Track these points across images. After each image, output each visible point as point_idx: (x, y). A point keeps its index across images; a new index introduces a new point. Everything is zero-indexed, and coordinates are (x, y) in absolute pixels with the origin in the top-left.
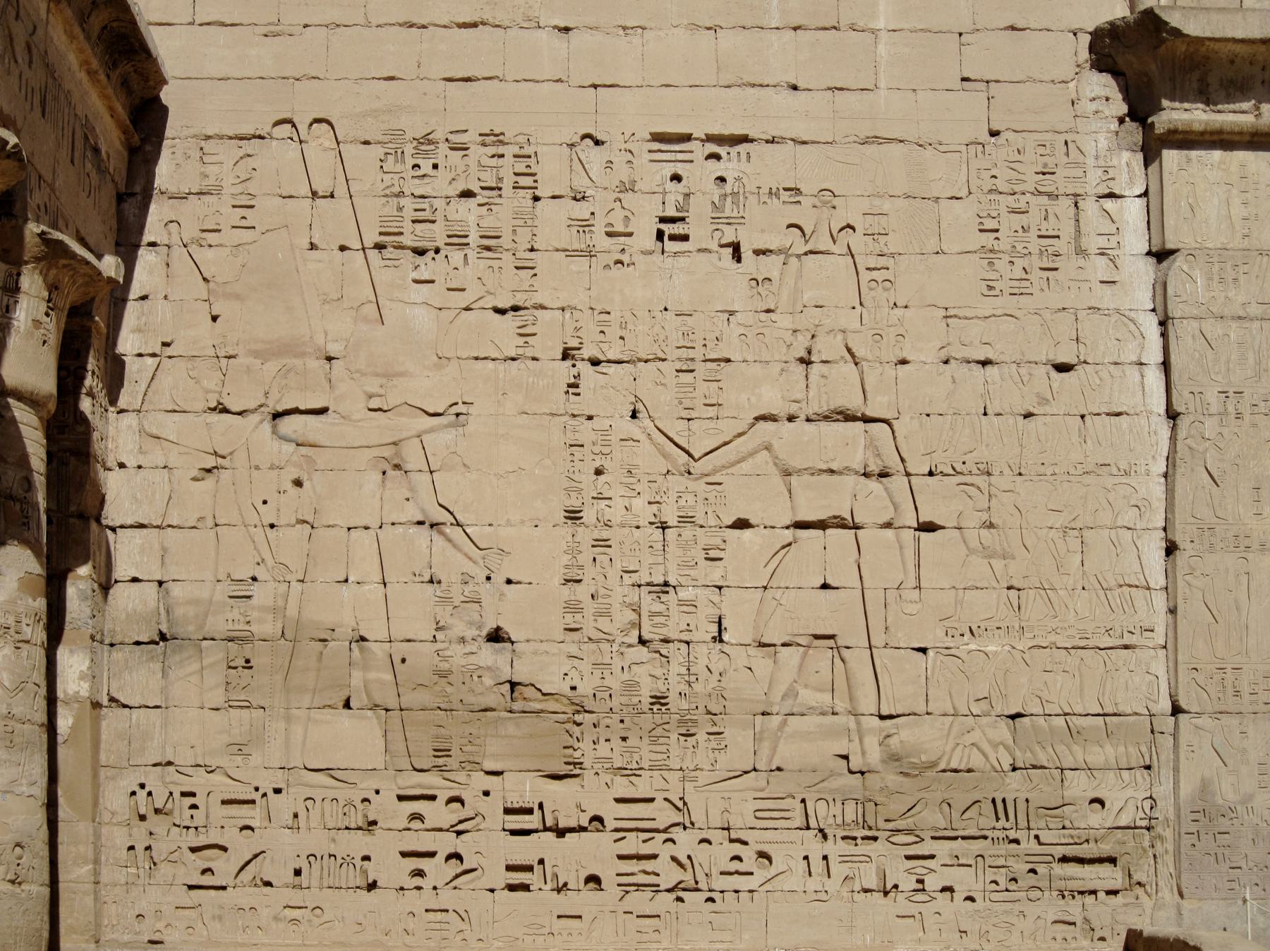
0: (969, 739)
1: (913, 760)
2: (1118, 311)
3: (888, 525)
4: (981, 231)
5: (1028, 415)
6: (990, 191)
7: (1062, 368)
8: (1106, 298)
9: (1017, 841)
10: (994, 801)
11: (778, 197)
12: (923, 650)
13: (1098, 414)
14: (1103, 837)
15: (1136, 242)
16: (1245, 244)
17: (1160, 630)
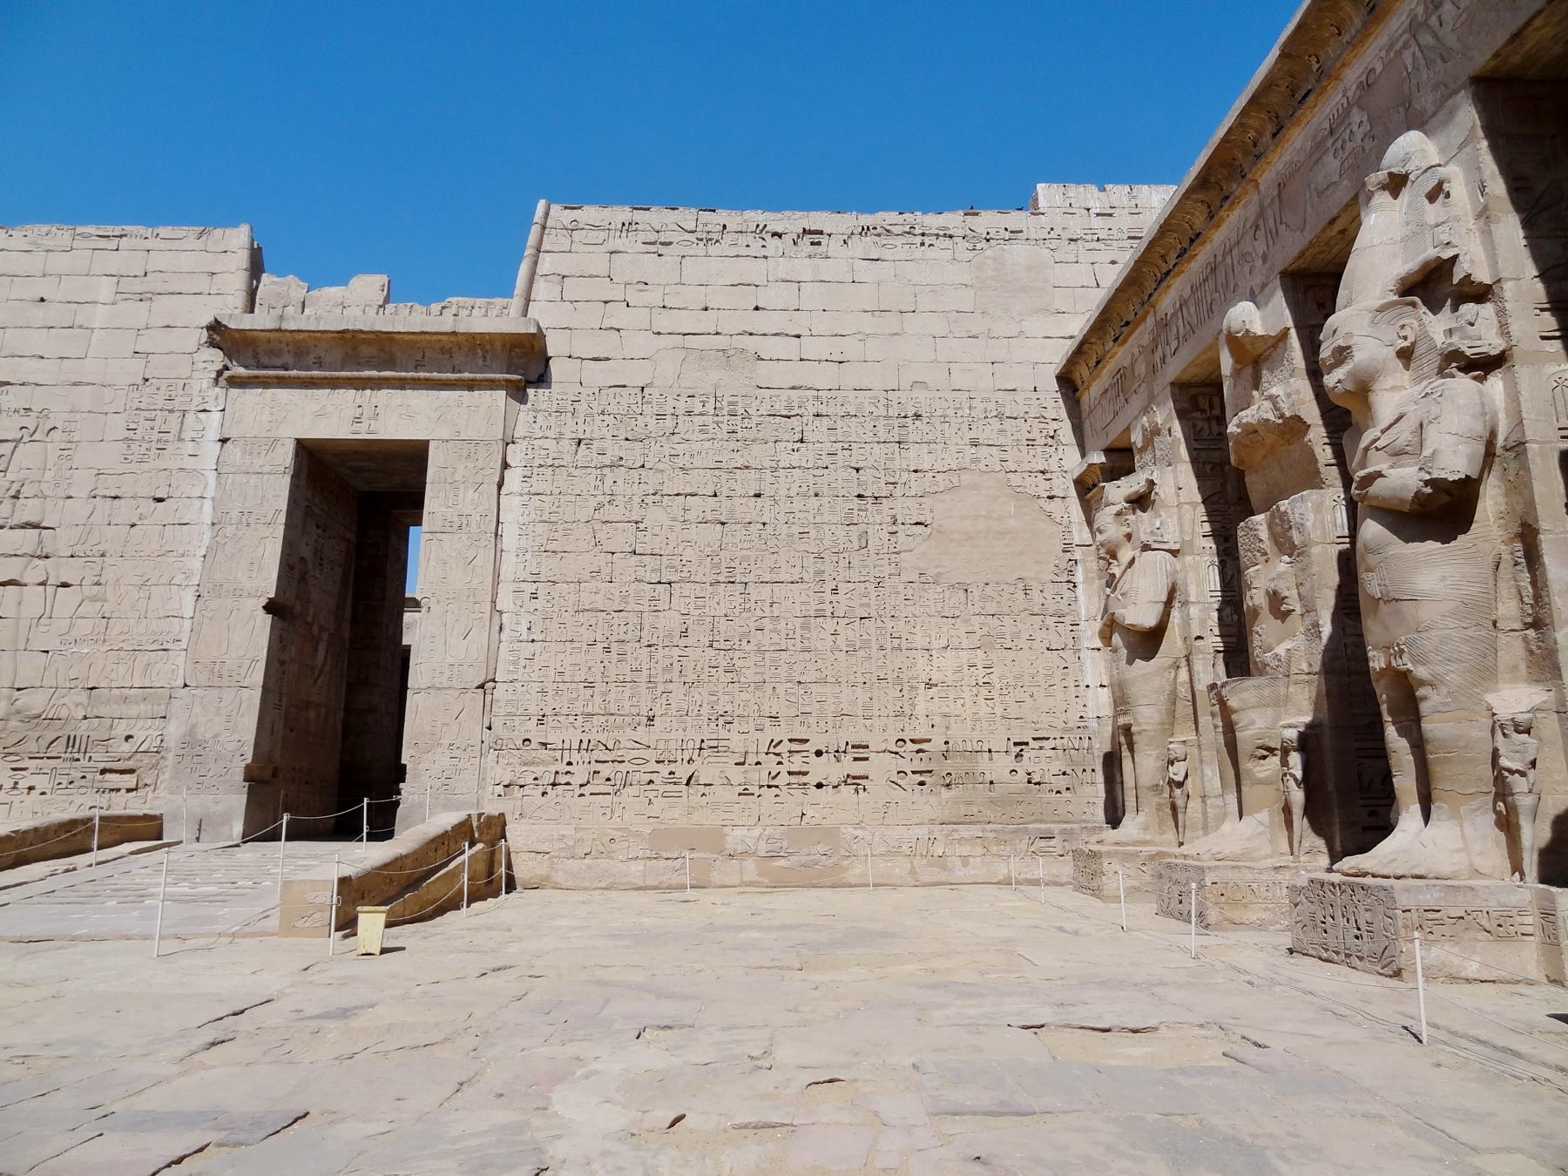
0: (63, 701)
1: (28, 713)
2: (195, 470)
3: (43, 584)
4: (128, 429)
5: (132, 526)
6: (136, 409)
7: (160, 500)
8: (190, 463)
9: (78, 760)
10: (69, 736)
11: (18, 412)
12: (47, 652)
13: (174, 524)
14: (129, 758)
15: (213, 434)
16: (268, 436)
17: (185, 641)
